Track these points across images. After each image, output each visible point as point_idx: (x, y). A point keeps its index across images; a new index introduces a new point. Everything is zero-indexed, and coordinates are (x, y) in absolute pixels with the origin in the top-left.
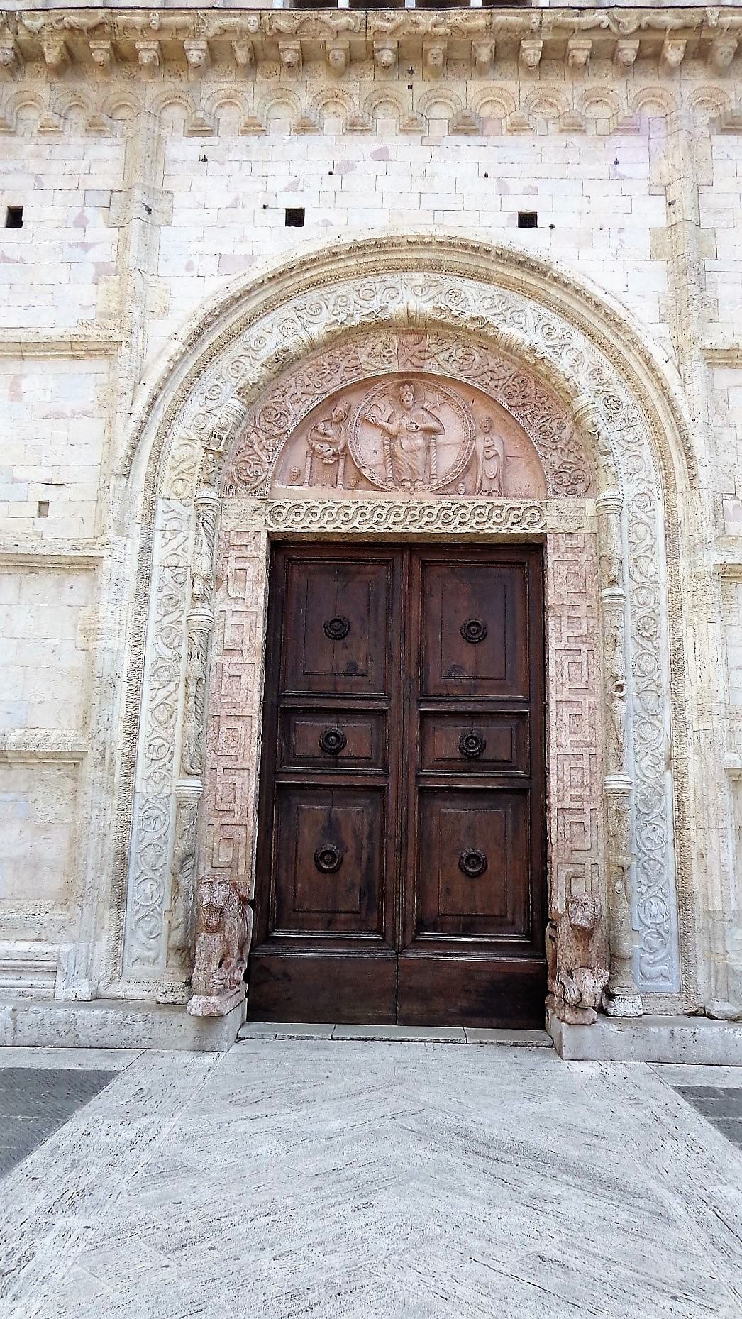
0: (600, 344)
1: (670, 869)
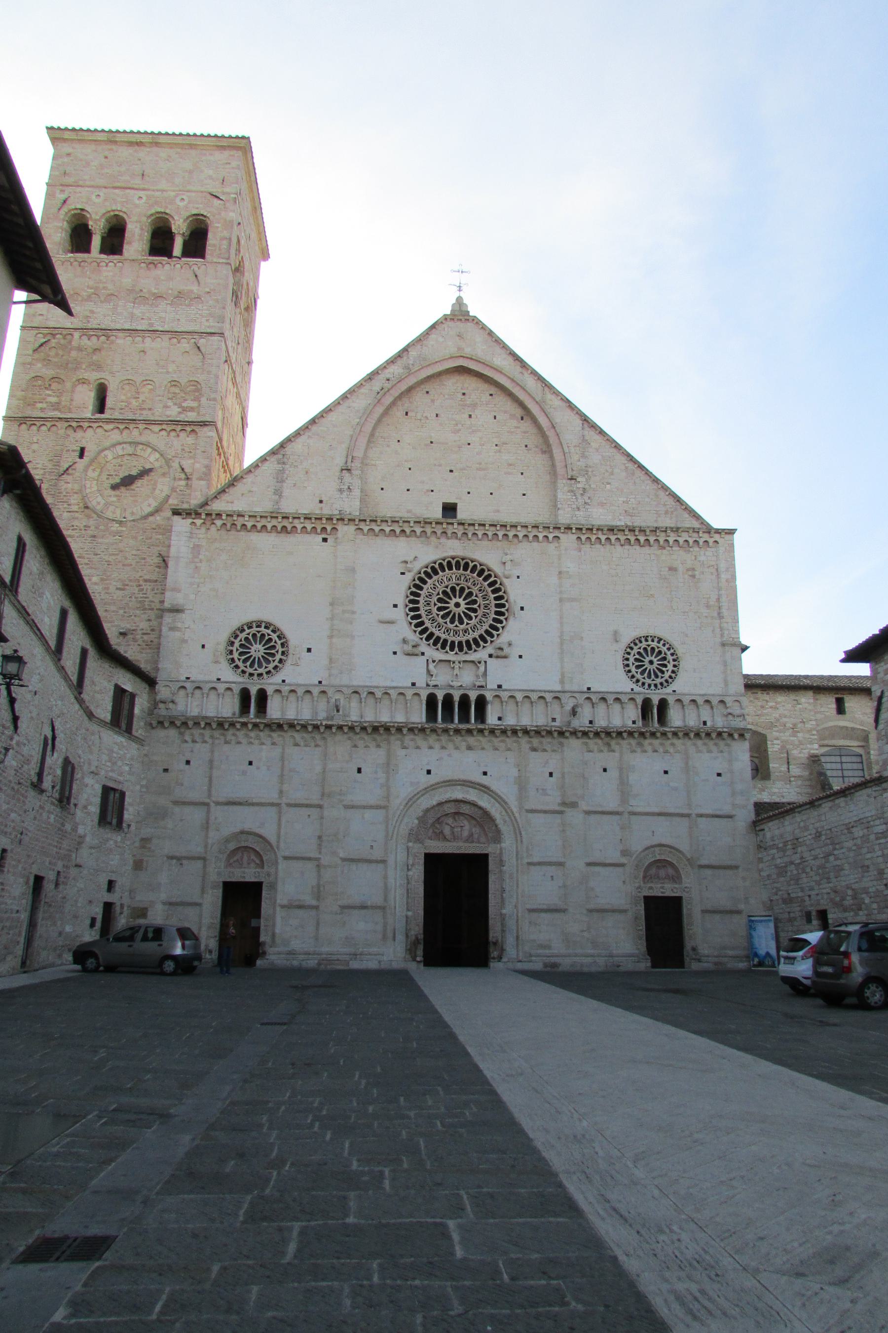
0: (502, 806)
1: (515, 931)
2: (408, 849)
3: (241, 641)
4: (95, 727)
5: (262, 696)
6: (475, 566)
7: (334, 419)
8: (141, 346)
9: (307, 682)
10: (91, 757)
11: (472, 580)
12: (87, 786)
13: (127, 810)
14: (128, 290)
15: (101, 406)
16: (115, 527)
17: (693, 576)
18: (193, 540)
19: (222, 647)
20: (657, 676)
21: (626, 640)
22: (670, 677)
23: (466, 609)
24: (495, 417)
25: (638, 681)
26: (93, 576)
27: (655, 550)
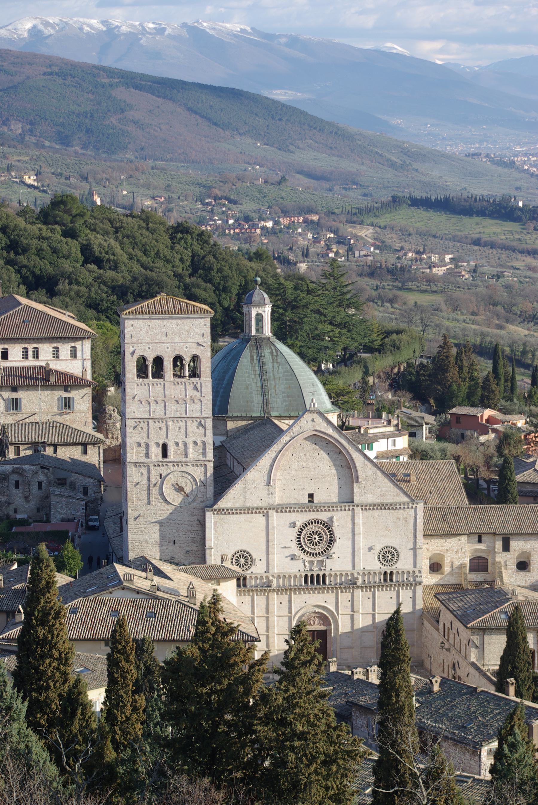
21: (378, 548)
27: (392, 511)
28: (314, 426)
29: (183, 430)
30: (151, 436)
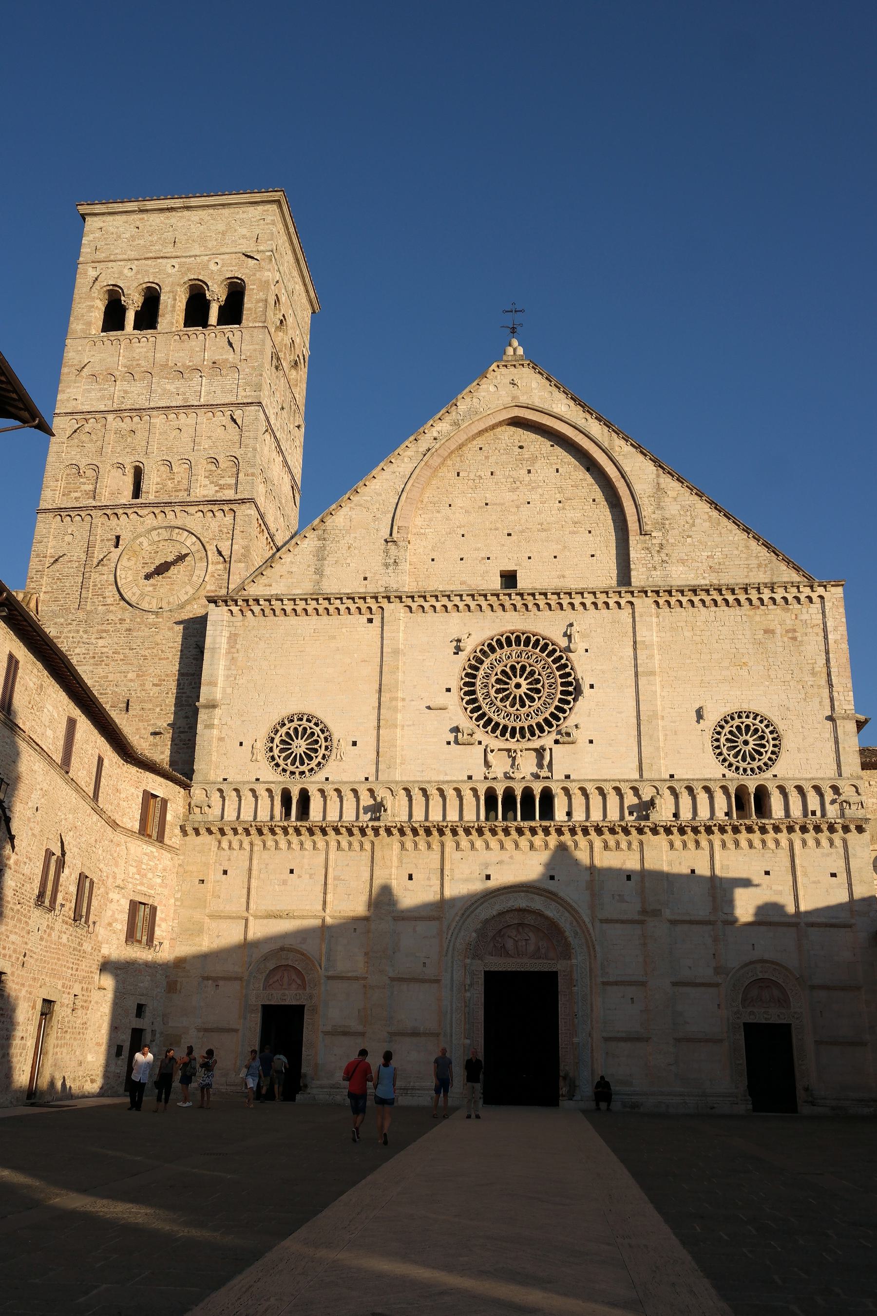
0: (573, 916)
2: (465, 967)
3: (281, 736)
4: (120, 838)
5: (305, 798)
6: (538, 641)
7: (377, 487)
8: (175, 423)
9: (352, 779)
10: (116, 870)
11: (534, 657)
12: (112, 901)
13: (159, 926)
14: (162, 365)
15: (137, 492)
16: (152, 618)
17: (794, 639)
18: (230, 629)
19: (261, 745)
20: (753, 759)
22: (770, 759)
23: (527, 689)
24: (557, 471)
25: (730, 765)
26: (128, 672)
28: (514, 398)
29: (186, 437)
30: (108, 449)
